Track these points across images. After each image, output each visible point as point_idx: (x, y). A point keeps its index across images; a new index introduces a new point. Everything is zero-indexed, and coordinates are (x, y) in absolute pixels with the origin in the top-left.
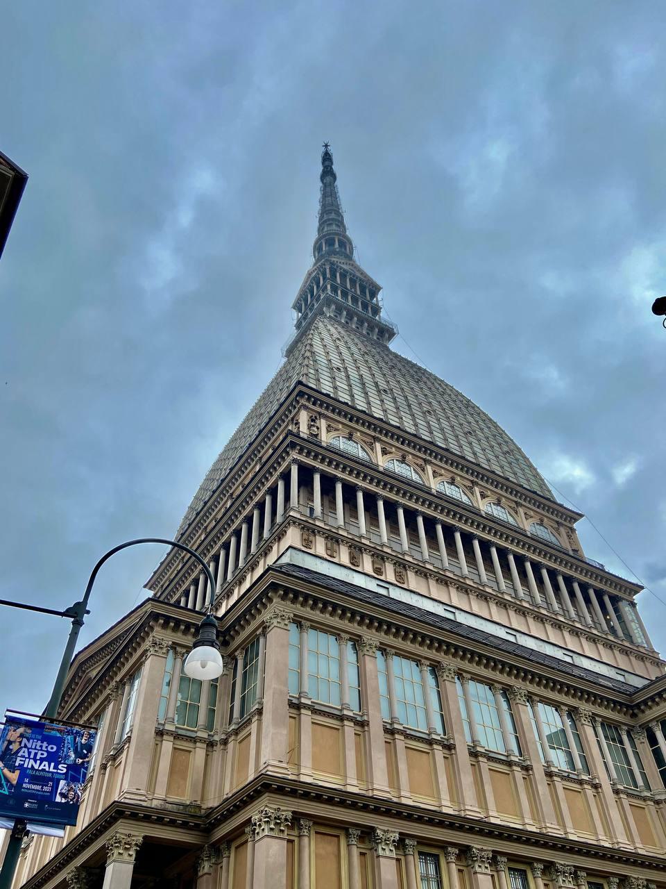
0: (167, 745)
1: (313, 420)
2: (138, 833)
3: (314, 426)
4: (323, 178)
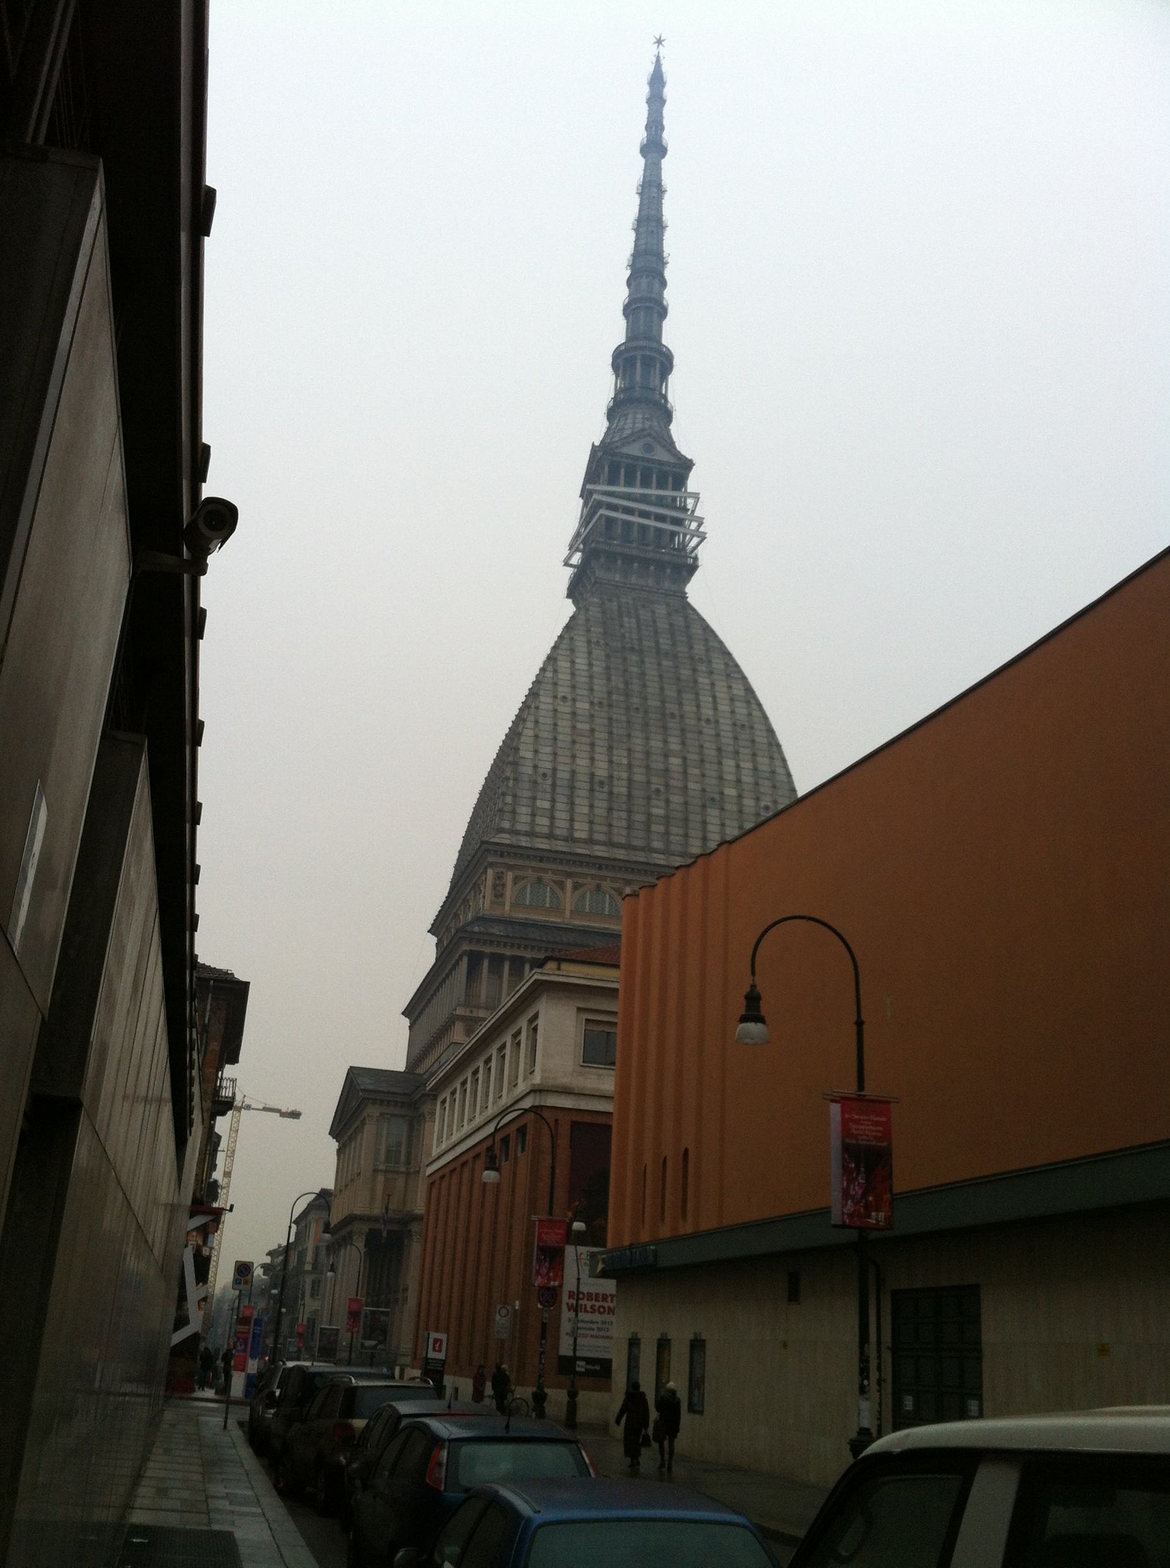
0: (381, 1178)
1: (499, 878)
2: (365, 1228)
3: (497, 885)
4: (645, 150)
